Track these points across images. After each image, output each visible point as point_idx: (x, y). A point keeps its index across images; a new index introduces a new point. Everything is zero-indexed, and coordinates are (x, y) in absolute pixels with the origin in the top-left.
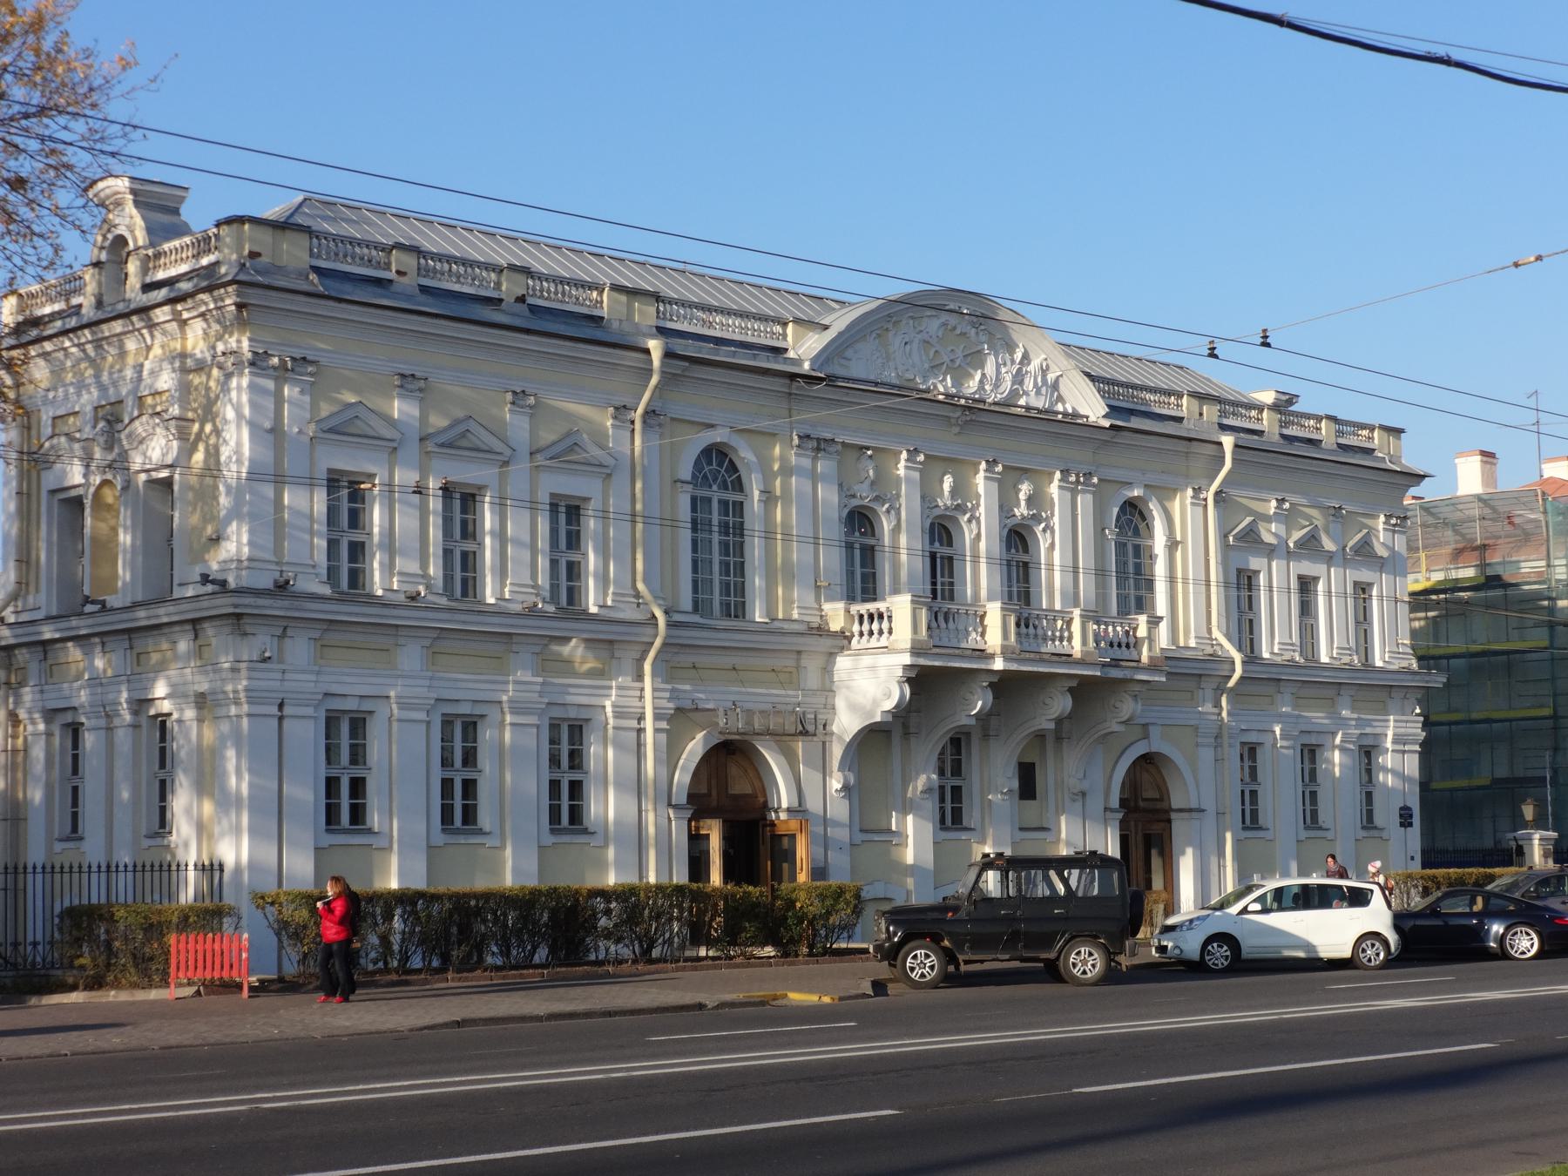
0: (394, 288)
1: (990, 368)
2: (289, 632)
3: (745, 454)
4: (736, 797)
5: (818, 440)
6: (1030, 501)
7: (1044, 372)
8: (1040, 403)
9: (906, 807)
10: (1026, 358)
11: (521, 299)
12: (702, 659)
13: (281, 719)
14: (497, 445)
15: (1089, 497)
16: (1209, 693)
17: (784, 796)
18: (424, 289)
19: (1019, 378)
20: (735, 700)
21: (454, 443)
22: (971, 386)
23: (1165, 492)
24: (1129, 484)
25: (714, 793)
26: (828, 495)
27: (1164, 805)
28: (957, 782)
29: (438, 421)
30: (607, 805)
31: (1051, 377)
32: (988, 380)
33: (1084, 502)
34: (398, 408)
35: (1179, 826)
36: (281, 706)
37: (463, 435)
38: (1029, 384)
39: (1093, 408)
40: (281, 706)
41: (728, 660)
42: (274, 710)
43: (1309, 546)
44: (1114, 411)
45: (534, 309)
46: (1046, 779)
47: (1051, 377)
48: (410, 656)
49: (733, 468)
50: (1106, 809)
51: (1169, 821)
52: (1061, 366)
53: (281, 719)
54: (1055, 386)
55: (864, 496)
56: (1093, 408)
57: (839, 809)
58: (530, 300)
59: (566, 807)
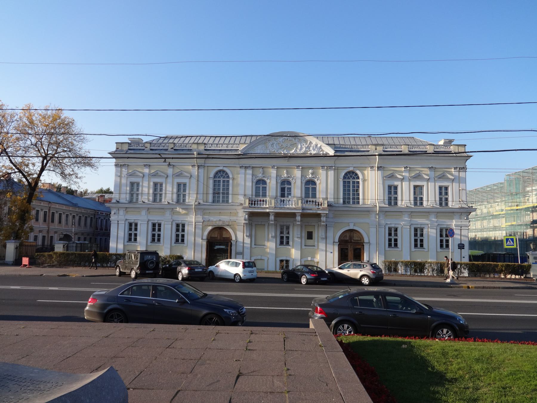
1: (299, 146)
3: (227, 170)
4: (224, 238)
5: (246, 167)
6: (312, 174)
7: (316, 145)
8: (315, 153)
9: (268, 240)
10: (311, 143)
11: (172, 148)
12: (211, 211)
14: (163, 175)
15: (332, 172)
16: (373, 215)
17: (234, 238)
18: (151, 149)
19: (308, 147)
20: (217, 219)
21: (155, 175)
22: (293, 151)
23: (362, 169)
24: (349, 167)
26: (249, 177)
27: (362, 241)
29: (152, 171)
30: (189, 238)
31: (319, 146)
32: (300, 149)
33: (331, 173)
34: (146, 171)
35: (366, 247)
38: (311, 148)
39: (331, 152)
41: (219, 211)
43: (418, 177)
44: (336, 151)
46: (315, 235)
47: (319, 146)
48: (144, 212)
49: (227, 174)
50: (334, 242)
52: (320, 144)
54: (320, 147)
55: (260, 176)
56: (331, 152)
57: (248, 241)
59: (180, 239)
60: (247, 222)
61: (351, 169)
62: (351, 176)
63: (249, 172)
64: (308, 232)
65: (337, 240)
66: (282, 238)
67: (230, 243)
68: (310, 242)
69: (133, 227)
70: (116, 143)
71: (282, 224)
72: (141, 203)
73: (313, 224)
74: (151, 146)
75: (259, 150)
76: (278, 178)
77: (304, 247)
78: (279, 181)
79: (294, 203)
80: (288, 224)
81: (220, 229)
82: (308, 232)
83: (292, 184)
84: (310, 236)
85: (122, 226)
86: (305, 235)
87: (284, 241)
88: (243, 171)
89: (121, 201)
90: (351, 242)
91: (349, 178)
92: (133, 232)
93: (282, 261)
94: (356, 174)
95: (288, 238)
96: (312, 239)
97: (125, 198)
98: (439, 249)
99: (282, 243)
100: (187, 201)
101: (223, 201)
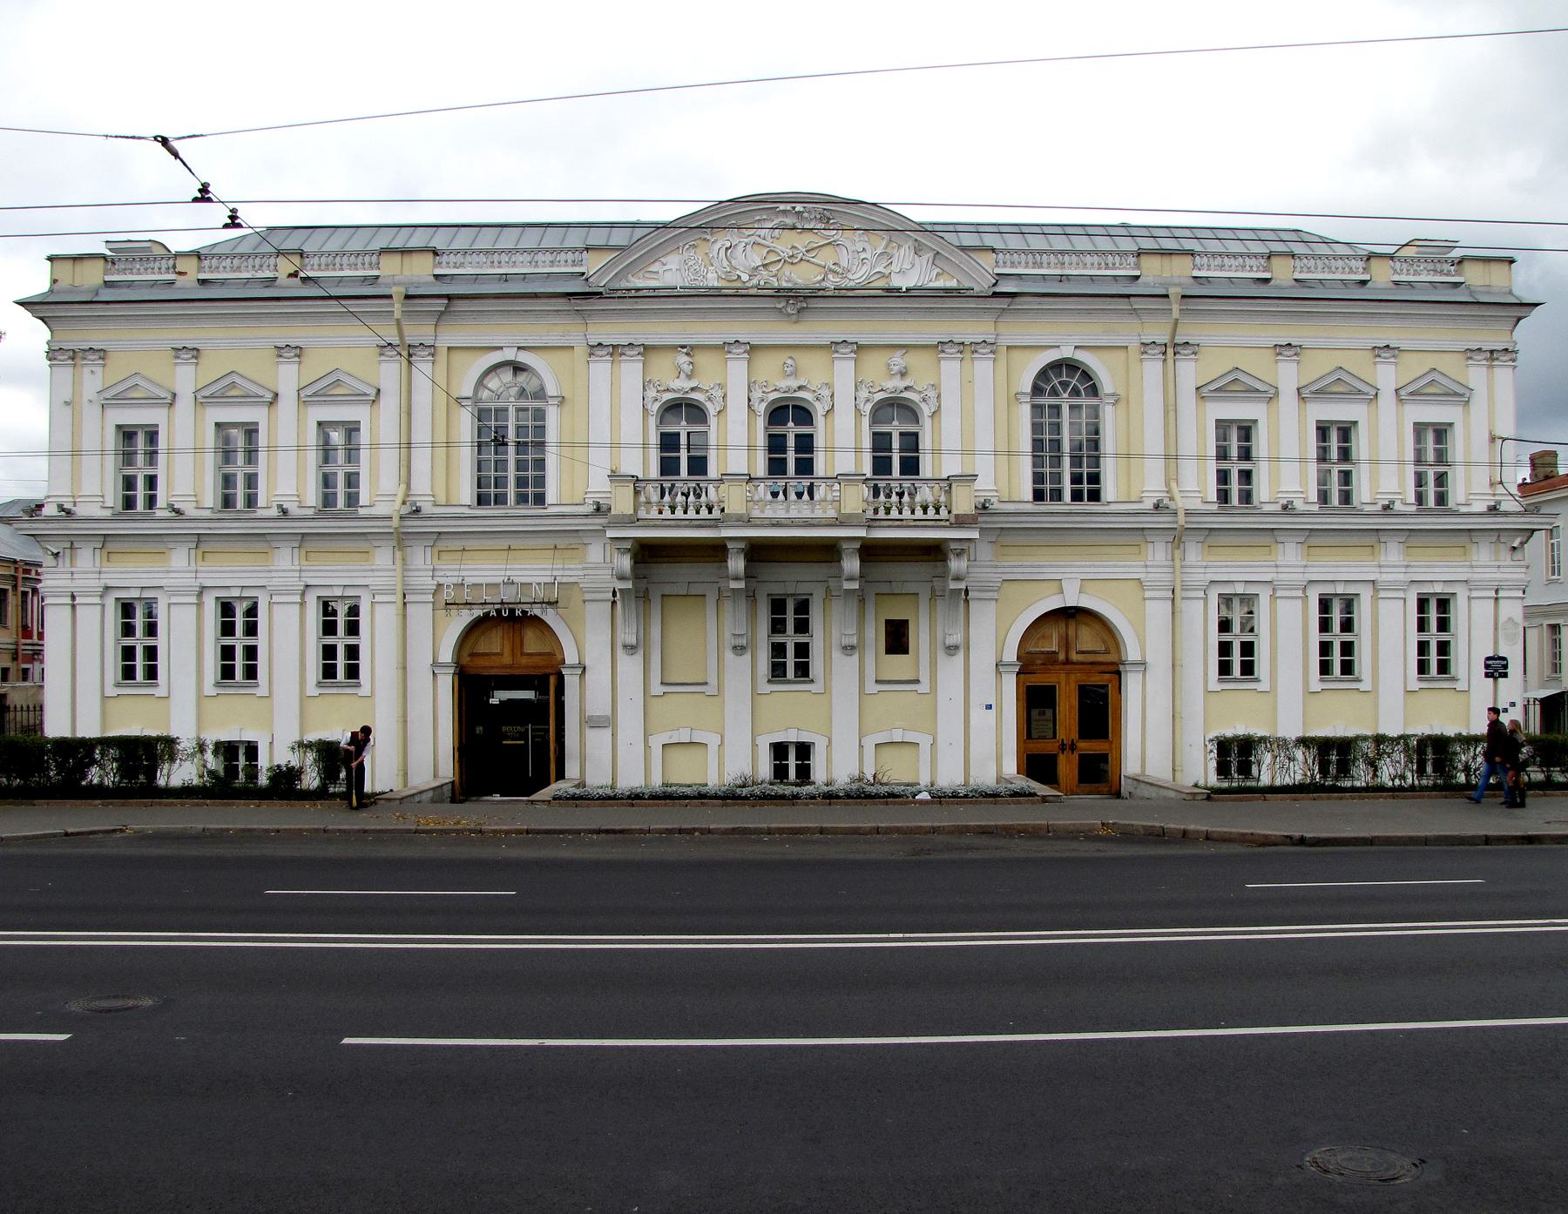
0: (178, 284)
2: (76, 545)
11: (295, 275)
13: (74, 606)
18: (203, 282)
25: (507, 652)
28: (802, 639)
36: (73, 597)
37: (233, 385)
40: (73, 597)
42: (69, 601)
45: (306, 280)
46: (919, 636)
51: (1119, 673)
53: (74, 606)
58: (302, 275)
60: (629, 585)
61: (1067, 352)
62: (1065, 385)
63: (631, 370)
64: (887, 622)
65: (1011, 655)
66: (778, 650)
67: (552, 680)
68: (898, 665)
69: (135, 617)
70: (51, 259)
71: (778, 590)
72: (166, 514)
73: (911, 588)
74: (200, 269)
75: (671, 271)
76: (757, 394)
77: (872, 687)
78: (761, 408)
79: (840, 499)
80: (803, 589)
81: (510, 619)
82: (887, 622)
83: (819, 420)
84: (897, 639)
85: (89, 617)
86: (875, 635)
87: (791, 664)
88: (601, 369)
89: (81, 511)
90: (1068, 662)
91: (1054, 393)
92: (139, 641)
93: (779, 750)
94: (1087, 376)
95: (803, 650)
96: (904, 650)
97: (97, 490)
98: (1414, 684)
99: (778, 671)
100: (363, 500)
101: (522, 499)
